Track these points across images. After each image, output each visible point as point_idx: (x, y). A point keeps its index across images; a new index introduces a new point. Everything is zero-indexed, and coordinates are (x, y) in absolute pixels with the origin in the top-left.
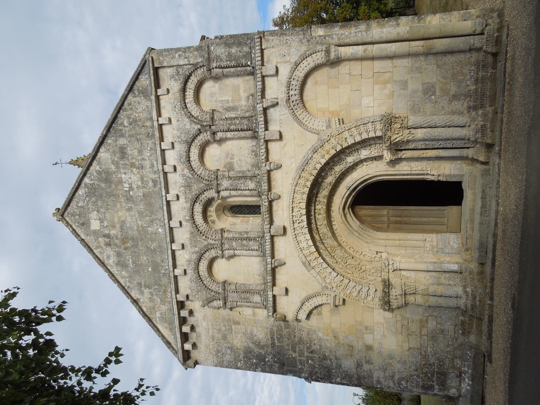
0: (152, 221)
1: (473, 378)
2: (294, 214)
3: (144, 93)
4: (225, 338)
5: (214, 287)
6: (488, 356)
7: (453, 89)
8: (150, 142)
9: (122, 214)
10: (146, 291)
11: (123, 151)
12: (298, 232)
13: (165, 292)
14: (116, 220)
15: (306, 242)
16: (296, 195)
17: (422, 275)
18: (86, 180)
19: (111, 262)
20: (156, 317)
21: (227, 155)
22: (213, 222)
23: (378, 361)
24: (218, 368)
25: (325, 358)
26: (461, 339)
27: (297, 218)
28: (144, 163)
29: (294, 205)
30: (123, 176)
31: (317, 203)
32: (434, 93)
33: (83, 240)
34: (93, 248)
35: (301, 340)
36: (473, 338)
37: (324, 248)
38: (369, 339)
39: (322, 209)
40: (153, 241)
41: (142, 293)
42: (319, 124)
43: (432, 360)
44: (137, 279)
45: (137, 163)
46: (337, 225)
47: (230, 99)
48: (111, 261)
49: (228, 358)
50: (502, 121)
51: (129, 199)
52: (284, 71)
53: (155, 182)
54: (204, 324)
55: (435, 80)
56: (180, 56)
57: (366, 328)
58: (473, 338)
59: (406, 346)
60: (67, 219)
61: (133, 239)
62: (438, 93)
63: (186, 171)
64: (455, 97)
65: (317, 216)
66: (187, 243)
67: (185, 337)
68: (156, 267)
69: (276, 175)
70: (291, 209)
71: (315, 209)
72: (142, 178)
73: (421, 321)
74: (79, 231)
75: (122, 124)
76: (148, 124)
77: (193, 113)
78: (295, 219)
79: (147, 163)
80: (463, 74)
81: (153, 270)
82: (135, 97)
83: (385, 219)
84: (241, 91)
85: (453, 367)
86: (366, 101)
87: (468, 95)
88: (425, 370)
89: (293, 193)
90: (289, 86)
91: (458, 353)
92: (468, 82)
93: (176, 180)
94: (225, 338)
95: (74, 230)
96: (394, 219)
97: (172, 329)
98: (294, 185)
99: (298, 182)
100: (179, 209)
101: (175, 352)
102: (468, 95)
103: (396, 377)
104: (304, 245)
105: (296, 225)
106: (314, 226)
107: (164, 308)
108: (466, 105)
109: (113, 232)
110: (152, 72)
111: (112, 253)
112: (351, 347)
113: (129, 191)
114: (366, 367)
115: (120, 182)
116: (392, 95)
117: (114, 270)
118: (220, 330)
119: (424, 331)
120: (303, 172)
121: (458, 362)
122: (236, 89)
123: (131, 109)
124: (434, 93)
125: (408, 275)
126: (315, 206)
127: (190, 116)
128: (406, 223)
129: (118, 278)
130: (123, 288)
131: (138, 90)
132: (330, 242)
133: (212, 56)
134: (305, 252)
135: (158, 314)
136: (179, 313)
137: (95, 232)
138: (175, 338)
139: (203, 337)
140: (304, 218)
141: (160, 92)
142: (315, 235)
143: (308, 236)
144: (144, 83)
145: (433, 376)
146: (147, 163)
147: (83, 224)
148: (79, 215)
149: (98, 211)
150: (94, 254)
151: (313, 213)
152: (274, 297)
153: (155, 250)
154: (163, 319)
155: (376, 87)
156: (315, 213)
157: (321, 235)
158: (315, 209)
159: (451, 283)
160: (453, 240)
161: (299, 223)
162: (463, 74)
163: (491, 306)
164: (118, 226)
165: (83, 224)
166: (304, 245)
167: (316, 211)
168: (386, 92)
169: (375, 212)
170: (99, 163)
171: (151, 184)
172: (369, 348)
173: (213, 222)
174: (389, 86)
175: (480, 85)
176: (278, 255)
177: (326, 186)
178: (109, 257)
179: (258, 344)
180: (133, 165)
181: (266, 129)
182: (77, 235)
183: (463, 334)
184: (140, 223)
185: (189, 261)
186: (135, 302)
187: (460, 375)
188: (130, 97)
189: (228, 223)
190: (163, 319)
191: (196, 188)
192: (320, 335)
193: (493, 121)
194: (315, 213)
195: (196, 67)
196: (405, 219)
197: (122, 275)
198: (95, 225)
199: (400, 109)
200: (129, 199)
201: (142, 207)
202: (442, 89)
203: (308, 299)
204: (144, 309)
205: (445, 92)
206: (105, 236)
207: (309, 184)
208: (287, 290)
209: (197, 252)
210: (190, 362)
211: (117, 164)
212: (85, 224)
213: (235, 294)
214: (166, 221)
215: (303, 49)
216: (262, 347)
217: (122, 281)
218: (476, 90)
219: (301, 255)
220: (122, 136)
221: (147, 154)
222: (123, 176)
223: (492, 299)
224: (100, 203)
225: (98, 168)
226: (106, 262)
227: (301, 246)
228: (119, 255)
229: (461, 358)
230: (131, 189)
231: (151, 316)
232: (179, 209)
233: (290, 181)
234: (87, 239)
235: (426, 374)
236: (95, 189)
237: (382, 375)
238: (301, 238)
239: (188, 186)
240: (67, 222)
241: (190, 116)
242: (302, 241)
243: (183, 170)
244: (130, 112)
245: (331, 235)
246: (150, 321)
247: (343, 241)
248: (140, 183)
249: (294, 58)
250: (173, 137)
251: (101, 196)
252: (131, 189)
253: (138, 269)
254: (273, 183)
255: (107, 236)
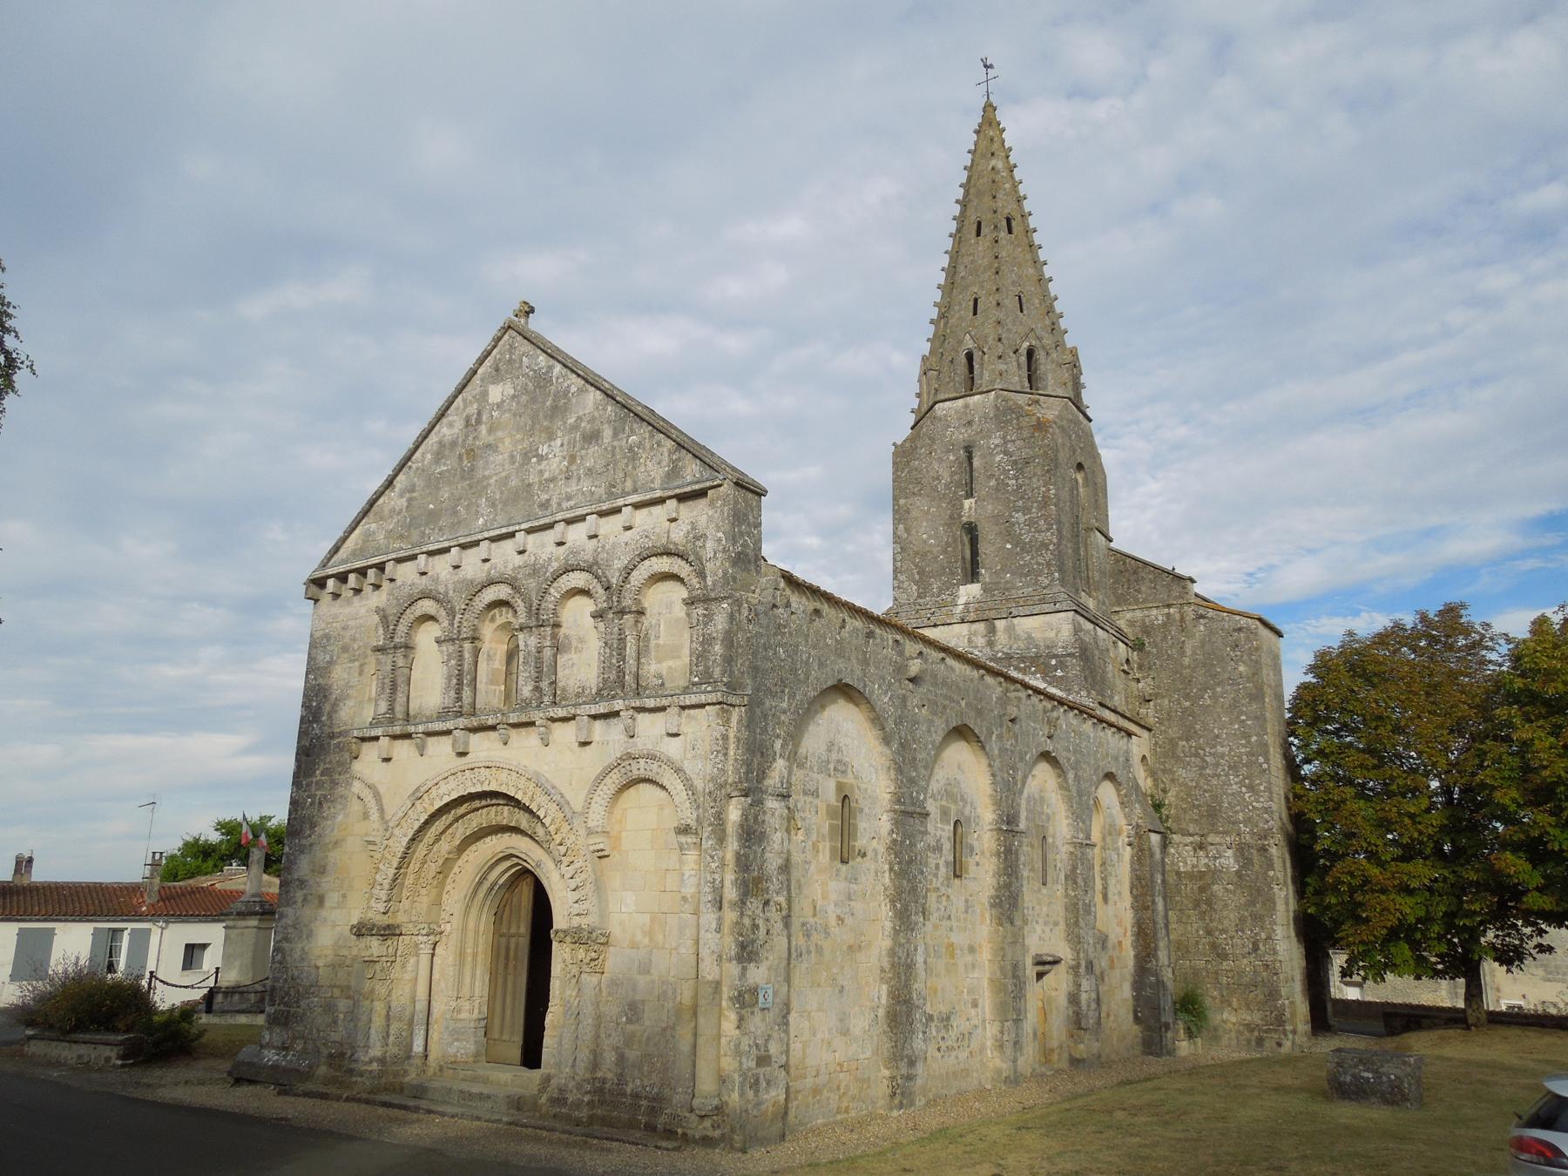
0: (493, 505)
1: (275, 1067)
3: (674, 472)
4: (345, 649)
5: (402, 628)
6: (284, 1090)
7: (632, 1054)
8: (602, 491)
9: (507, 445)
10: (403, 502)
11: (592, 437)
13: (401, 537)
14: (500, 434)
17: (407, 989)
18: (558, 368)
19: (444, 431)
20: (368, 525)
21: (581, 640)
22: (493, 619)
23: (307, 911)
24: (308, 640)
25: (313, 826)
26: (325, 1052)
28: (574, 480)
30: (559, 442)
32: (629, 1021)
33: (475, 372)
34: (464, 394)
35: (334, 783)
36: (323, 1070)
38: (332, 898)
40: (468, 508)
41: (401, 496)
42: (596, 816)
43: (303, 1003)
44: (419, 483)
45: (574, 467)
47: (661, 642)
48: (445, 430)
49: (322, 658)
50: (553, 1130)
51: (526, 456)
52: (673, 748)
53: (545, 505)
54: (363, 611)
55: (647, 1023)
56: (719, 540)
57: (344, 896)
58: (323, 1070)
59: (320, 963)
60: (506, 337)
61: (472, 469)
62: (630, 1027)
63: (555, 565)
64: (621, 1058)
66: (461, 573)
67: (342, 578)
68: (433, 517)
69: (529, 739)
72: (553, 480)
73: (349, 987)
74: (488, 363)
75: (632, 432)
76: (629, 485)
77: (634, 573)
79: (573, 488)
80: (650, 1072)
81: (431, 513)
82: (670, 453)
83: (513, 931)
84: (670, 663)
85: (294, 1038)
86: (630, 898)
87: (621, 1078)
88: (292, 993)
90: (652, 757)
91: (310, 1047)
92: (638, 1082)
93: (542, 547)
94: (345, 649)
95: (489, 353)
96: (513, 946)
97: (355, 554)
100: (505, 556)
101: (324, 565)
102: (621, 1078)
103: (285, 945)
106: (477, 804)
107: (381, 537)
108: (609, 1076)
109: (483, 429)
110: (697, 487)
111: (456, 431)
112: (323, 871)
113: (537, 456)
114: (299, 895)
115: (551, 437)
116: (634, 945)
117: (433, 438)
118: (354, 640)
119: (337, 992)
121: (299, 1046)
122: (673, 653)
123: (652, 448)
124: (629, 1021)
125: (409, 968)
127: (628, 571)
128: (506, 967)
129: (420, 450)
130: (408, 458)
131: (679, 459)
133: (713, 606)
135: (374, 526)
136: (371, 567)
137: (485, 394)
138: (344, 562)
139: (347, 610)
140: (479, 789)
141: (672, 503)
144: (689, 471)
145: (286, 1004)
146: (573, 488)
147: (497, 370)
148: (510, 360)
149: (514, 397)
150: (456, 397)
152: (376, 738)
153: (455, 513)
154: (368, 535)
155: (647, 917)
159: (392, 1038)
160: (466, 1047)
162: (650, 1072)
163: (338, 1098)
164: (491, 439)
165: (497, 370)
168: (639, 937)
169: (523, 913)
170: (580, 391)
171: (545, 497)
172: (321, 900)
173: (493, 619)
174: (646, 941)
175: (629, 1101)
176: (431, 741)
178: (451, 425)
179: (335, 708)
180: (572, 459)
181: (595, 717)
182: (481, 361)
183: (331, 1056)
184: (492, 481)
185: (436, 580)
186: (389, 483)
187: (284, 1048)
188: (669, 444)
189: (494, 645)
190: (368, 535)
191: (532, 584)
192: (340, 818)
193: (568, 1118)
195: (701, 574)
196: (511, 966)
197: (425, 456)
198: (496, 393)
199: (614, 961)
200: (526, 456)
201: (514, 482)
202: (633, 1035)
203: (377, 796)
204: (381, 501)
205: (629, 1040)
206: (479, 413)
208: (387, 760)
209: (447, 593)
210: (314, 588)
211: (575, 428)
212: (497, 375)
213: (389, 668)
214: (486, 535)
215: (699, 784)
216: (330, 717)
217: (418, 455)
218: (624, 1095)
219: (430, 784)
220: (615, 435)
221: (586, 485)
222: (559, 442)
223: (348, 1099)
224: (524, 398)
225: (573, 389)
226: (444, 420)
228: (454, 444)
229: (304, 1051)
230: (541, 458)
231: (371, 514)
232: (505, 556)
234: (476, 380)
235: (287, 994)
236: (545, 387)
237: (290, 922)
238: (452, 783)
239: (535, 571)
240: (499, 339)
241: (628, 571)
243: (557, 559)
244: (648, 446)
246: (365, 513)
248: (546, 475)
249: (688, 767)
250: (606, 536)
251: (533, 400)
252: (541, 458)
253: (433, 483)
254: (523, 731)
255: (479, 422)
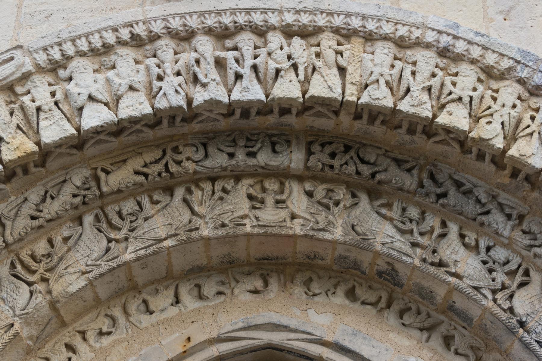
2: (275, 40)
12: (167, 55)
15: (104, 96)
16: (383, 53)
27: (248, 51)
29: (328, 42)
31: (320, 191)
37: (52, 208)
39: (284, 214)
46: (174, 311)
65: (245, 186)
70: (305, 19)
71: (283, 176)
78: (246, 41)
89: (402, 31)
98: (445, 40)
99: (464, 68)
104: (86, 80)
105: (205, 46)
120: (518, 89)
126: (300, 179)
132: (84, 258)
134: (41, 91)
140: (251, 91)
142: (136, 163)
143: (135, 106)
151: (264, 158)
156: (263, 174)
157: (129, 206)
158: (283, 176)
161: (220, 63)
166: (86, 80)
167: (271, 185)
177: (424, 241)
194: (263, 174)
207: (456, 118)
227: (76, 64)
233: (468, 26)
238: (127, 67)
242: (111, 74)
245: (128, 256)
247: (77, 341)
